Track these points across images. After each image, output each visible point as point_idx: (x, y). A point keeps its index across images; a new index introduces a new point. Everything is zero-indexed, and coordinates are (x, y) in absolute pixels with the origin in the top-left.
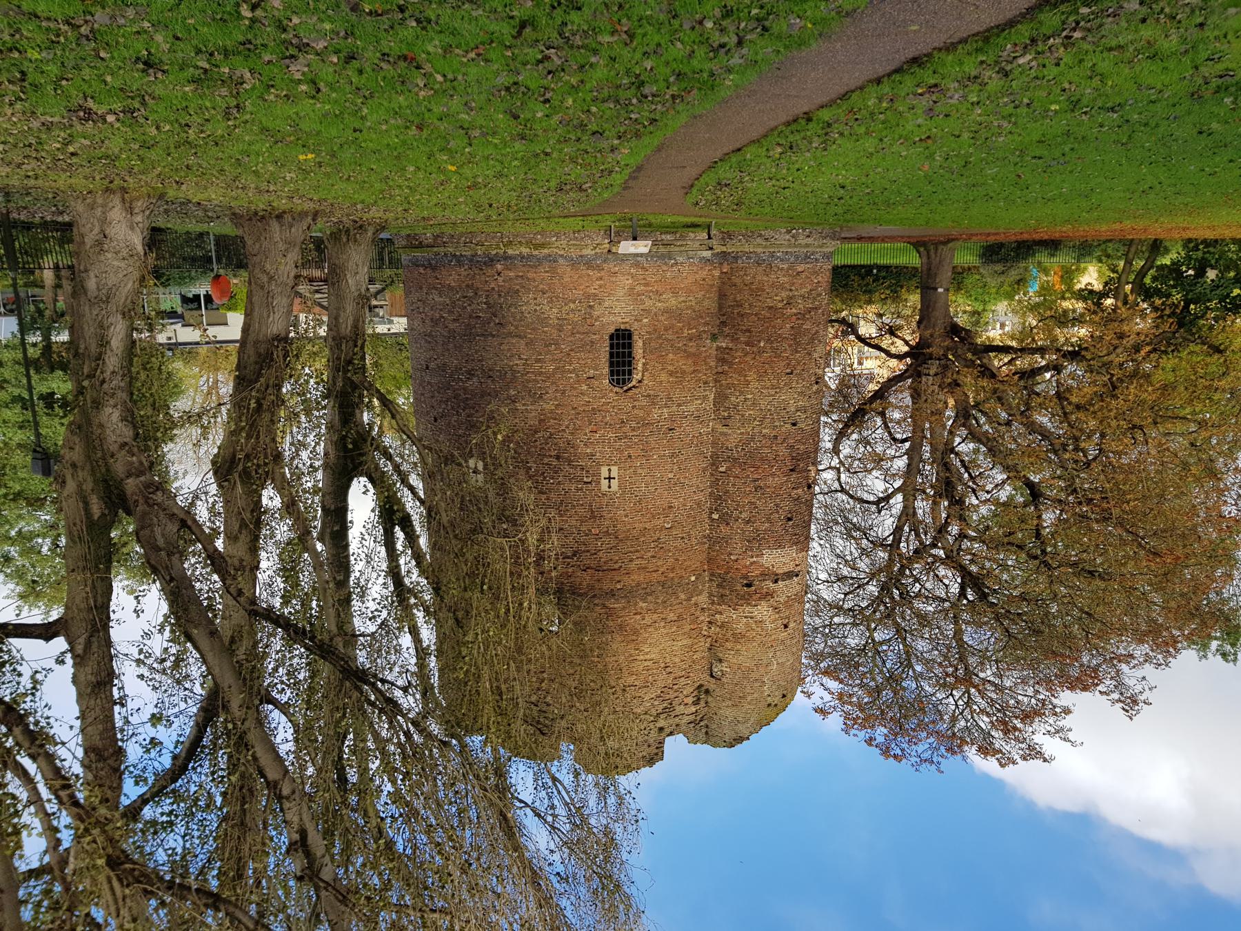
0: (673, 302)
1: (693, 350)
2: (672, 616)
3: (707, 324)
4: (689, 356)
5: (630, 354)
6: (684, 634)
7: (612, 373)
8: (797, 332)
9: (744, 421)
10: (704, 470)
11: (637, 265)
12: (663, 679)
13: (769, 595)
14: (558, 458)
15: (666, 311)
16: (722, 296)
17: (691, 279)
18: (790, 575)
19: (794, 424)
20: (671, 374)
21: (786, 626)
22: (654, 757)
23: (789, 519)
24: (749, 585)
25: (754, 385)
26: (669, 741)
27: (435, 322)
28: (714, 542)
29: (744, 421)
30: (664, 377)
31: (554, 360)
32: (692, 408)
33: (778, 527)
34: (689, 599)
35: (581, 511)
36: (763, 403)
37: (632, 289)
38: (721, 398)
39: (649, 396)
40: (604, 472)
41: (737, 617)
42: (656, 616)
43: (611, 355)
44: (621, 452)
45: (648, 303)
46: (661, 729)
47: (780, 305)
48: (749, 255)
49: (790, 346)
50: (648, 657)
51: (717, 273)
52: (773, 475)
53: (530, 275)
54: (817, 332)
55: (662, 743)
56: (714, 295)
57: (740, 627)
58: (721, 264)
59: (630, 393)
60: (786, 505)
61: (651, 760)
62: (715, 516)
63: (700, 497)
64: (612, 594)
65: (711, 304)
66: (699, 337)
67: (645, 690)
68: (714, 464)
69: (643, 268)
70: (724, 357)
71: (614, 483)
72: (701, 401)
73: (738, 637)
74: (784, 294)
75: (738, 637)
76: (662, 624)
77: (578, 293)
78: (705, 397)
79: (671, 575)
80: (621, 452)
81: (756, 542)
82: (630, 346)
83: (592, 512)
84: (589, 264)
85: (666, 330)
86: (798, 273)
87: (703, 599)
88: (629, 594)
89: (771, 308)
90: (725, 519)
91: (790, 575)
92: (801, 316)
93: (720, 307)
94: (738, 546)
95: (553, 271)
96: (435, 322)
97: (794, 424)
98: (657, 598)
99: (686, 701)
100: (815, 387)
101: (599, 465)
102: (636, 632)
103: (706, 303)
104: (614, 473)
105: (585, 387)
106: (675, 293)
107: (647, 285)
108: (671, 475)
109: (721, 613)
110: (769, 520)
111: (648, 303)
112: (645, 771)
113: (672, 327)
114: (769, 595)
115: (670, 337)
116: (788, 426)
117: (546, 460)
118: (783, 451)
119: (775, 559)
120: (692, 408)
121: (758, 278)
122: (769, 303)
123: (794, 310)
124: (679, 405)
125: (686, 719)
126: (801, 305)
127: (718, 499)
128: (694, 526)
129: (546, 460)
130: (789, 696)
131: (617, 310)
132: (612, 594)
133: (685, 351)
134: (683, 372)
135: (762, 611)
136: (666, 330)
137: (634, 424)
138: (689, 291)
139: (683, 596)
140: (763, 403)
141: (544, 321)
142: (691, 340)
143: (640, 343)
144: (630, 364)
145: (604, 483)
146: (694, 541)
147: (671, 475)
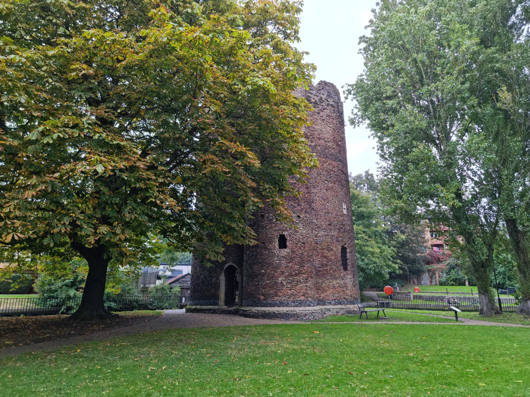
0: (334, 282)
2: (322, 141)
3: (320, 271)
4: (326, 257)
6: (317, 131)
7: (346, 252)
10: (313, 202)
11: (347, 300)
15: (336, 278)
17: (328, 293)
19: (298, 216)
30: (335, 249)
32: (321, 233)
34: (316, 145)
39: (339, 242)
46: (323, 94)
49: (304, 257)
50: (329, 128)
54: (290, 262)
61: (326, 83)
66: (322, 265)
69: (344, 298)
74: (308, 284)
76: (326, 139)
78: (316, 237)
79: (324, 159)
89: (312, 278)
92: (300, 273)
97: (298, 216)
98: (328, 152)
100: (286, 233)
106: (334, 288)
107: (343, 291)
111: (342, 283)
113: (334, 272)
116: (302, 216)
118: (303, 204)
124: (328, 235)
125: (314, 92)
126: (302, 278)
128: (315, 178)
133: (328, 259)
134: (327, 250)
136: (336, 270)
139: (319, 148)
142: (326, 264)
147: (328, 204)
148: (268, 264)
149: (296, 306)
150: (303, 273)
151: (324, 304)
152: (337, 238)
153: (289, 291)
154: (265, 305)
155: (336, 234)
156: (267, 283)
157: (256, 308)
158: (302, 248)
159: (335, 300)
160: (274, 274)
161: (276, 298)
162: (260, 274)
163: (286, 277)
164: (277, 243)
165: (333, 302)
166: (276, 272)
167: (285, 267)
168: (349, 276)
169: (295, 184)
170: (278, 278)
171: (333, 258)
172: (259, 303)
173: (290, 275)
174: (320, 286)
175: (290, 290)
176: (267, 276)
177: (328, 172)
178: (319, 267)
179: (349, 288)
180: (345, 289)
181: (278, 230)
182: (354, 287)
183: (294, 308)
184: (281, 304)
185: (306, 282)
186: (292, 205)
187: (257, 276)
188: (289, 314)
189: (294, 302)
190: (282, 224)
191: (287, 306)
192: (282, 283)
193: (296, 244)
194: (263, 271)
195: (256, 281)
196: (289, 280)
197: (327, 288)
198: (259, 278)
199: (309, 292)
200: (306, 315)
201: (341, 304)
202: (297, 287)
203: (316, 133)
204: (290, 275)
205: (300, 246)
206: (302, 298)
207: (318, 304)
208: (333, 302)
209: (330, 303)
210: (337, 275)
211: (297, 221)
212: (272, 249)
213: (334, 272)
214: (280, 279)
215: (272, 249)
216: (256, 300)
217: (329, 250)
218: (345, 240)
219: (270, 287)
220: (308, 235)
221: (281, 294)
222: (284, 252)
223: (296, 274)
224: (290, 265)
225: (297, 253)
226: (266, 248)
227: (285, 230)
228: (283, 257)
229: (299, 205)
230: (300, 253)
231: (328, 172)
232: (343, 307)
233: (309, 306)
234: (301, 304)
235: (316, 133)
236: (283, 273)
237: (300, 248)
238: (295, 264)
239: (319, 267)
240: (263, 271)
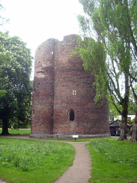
1: (58, 117)
5: (70, 116)
9: (48, 103)
10: (55, 93)
11: (69, 132)
12: (64, 52)
13: (43, 69)
14: (84, 97)
15: (63, 124)
16: (53, 127)
17: (58, 130)
18: (39, 72)
20: (62, 112)
21: (39, 62)
22: (66, 38)
23: (39, 84)
24: (47, 71)
25: (46, 110)
26: (62, 41)
27: (105, 122)
28: (53, 79)
29: (48, 103)
31: (85, 115)
32: (58, 106)
33: (41, 82)
34: (58, 68)
35: (80, 87)
36: (45, 106)
37: (70, 128)
38: (53, 107)
40: (75, 94)
41: (49, 64)
42: (65, 65)
43: (74, 116)
44: (72, 98)
46: (64, 43)
48: (48, 134)
51: (54, 131)
52: (42, 92)
53: (89, 131)
54: (34, 119)
55: (64, 40)
56: (54, 127)
57: (48, 62)
58: (53, 132)
59: (70, 109)
60: (40, 86)
62: (53, 84)
63: (56, 88)
64: (74, 70)
65: (54, 124)
67: (67, 51)
68: (53, 95)
70: (52, 115)
71: (73, 92)
72: (56, 107)
73: (49, 60)
75: (49, 60)
77: (80, 127)
79: (62, 73)
80: (72, 98)
81: (45, 79)
82: (70, 118)
83: (78, 86)
84: (78, 132)
87: (55, 68)
88: (70, 70)
90: (51, 84)
91: (39, 72)
92: (38, 122)
93: (53, 124)
94: (49, 79)
95: (85, 131)
96: (105, 122)
99: (59, 48)
100: (34, 109)
101: (76, 95)
102: (69, 62)
104: (73, 94)
105: (79, 110)
106: (62, 127)
108: (62, 93)
109: (52, 65)
110: (43, 83)
112: (67, 35)
113: (62, 121)
114: (43, 69)
115: (63, 119)
117: (86, 96)
118: (41, 97)
119: (42, 76)
120: (58, 106)
121: (46, 130)
122: (44, 125)
125: (59, 44)
127: (53, 88)
129: (86, 96)
130: (38, 48)
131: (73, 124)
132: (74, 70)
135: (44, 65)
137: (70, 103)
138: (59, 127)
139: (60, 69)
140: (45, 106)
141: (87, 123)
143: (69, 118)
145: (75, 92)
146: (57, 79)
147: (62, 93)
152: (66, 107)
155: (65, 105)
171: (63, 116)
173: (35, 124)
177: (64, 78)
182: (78, 127)
203: (59, 62)
204: (35, 124)
213: (62, 121)
217: (61, 112)
218: (71, 107)
220: (43, 108)
227: (34, 108)
231: (64, 78)
234: (37, 133)
235: (59, 62)
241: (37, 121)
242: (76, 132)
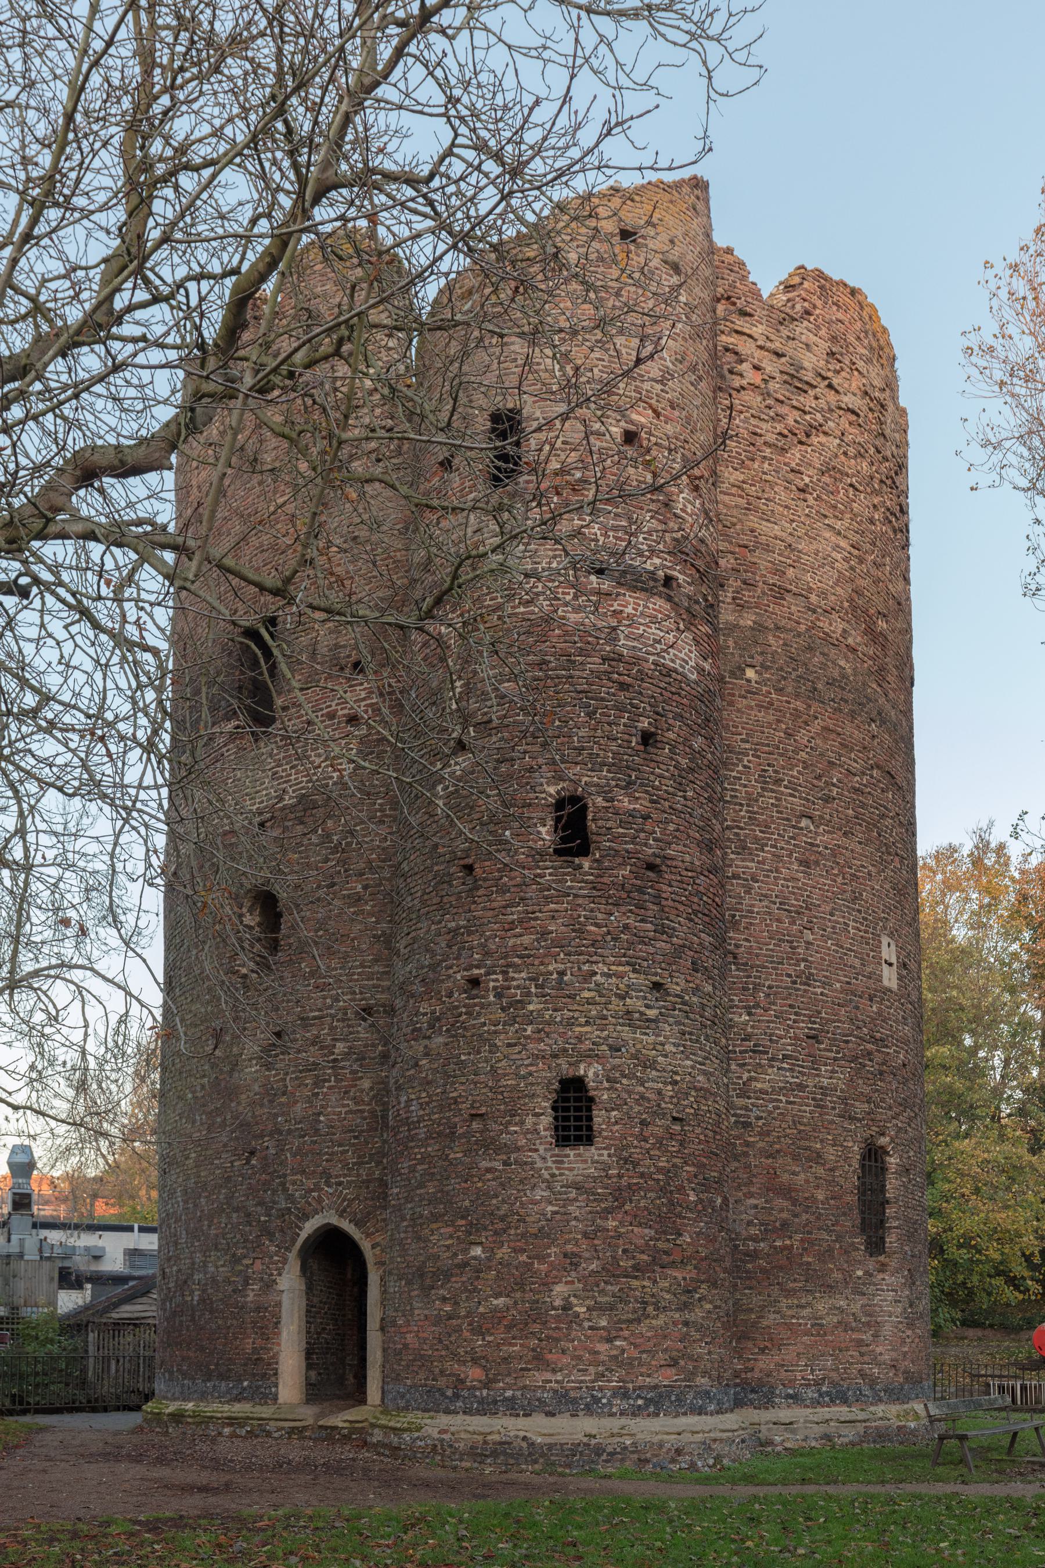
3: (754, 1255)
8: (667, 1223)
11: (872, 1382)
15: (830, 1289)
17: (789, 1354)
19: (657, 986)
37: (876, 1336)
45: (857, 1306)
47: (703, 1290)
54: (608, 1211)
74: (697, 1314)
85: (830, 1250)
86: (673, 1363)
89: (714, 1285)
97: (657, 986)
100: (591, 1072)
103: (756, 1300)
107: (860, 1343)
111: (856, 1308)
118: (681, 926)
123: (679, 1275)
126: (664, 1285)
142: (785, 1224)
144: (864, 1184)
148: (502, 1219)
149: (636, 1412)
150: (673, 1264)
151: (768, 1403)
153: (602, 1347)
154: (488, 1407)
156: (496, 1309)
157: (444, 1420)
158: (674, 1146)
159: (818, 1383)
160: (528, 1266)
161: (539, 1377)
162: (465, 1264)
163: (591, 1282)
164: (546, 1121)
165: (811, 1394)
166: (542, 1258)
167: (585, 1235)
168: (889, 1279)
169: (646, 817)
170: (547, 1285)
172: (457, 1396)
173: (611, 1272)
174: (754, 1324)
175: (610, 1340)
176: (499, 1277)
178: (755, 1239)
179: (887, 1330)
180: (867, 1337)
181: (555, 1056)
183: (624, 1421)
184: (565, 1402)
185: (685, 1307)
186: (626, 927)
187: (448, 1275)
188: (599, 1450)
189: (625, 1396)
190: (571, 1023)
191: (589, 1411)
192: (567, 1307)
193: (643, 1123)
194: (477, 1251)
195: (444, 1299)
196: (602, 1292)
197: (785, 1334)
198: (456, 1283)
199: (701, 1350)
200: (679, 1452)
201: (845, 1401)
202: (643, 1328)
204: (611, 1272)
205: (659, 1131)
206: (665, 1377)
207: (739, 1403)
208: (811, 1394)
209: (796, 1398)
210: (837, 1275)
211: (652, 1013)
212: (518, 1149)
214: (559, 1288)
215: (518, 1149)
216: (442, 1382)
219: (509, 1328)
221: (566, 1360)
222: (581, 1163)
223: (636, 1268)
224: (611, 1224)
225: (646, 1166)
226: (490, 1145)
227: (591, 1056)
228: (578, 1187)
229: (661, 930)
230: (660, 1170)
232: (855, 1412)
233: (701, 1411)
234: (656, 1402)
236: (572, 1260)
237: (660, 1143)
238: (636, 1219)
239: (755, 1239)
240: (477, 1251)
241: (642, 1234)
242: (908, 1375)
